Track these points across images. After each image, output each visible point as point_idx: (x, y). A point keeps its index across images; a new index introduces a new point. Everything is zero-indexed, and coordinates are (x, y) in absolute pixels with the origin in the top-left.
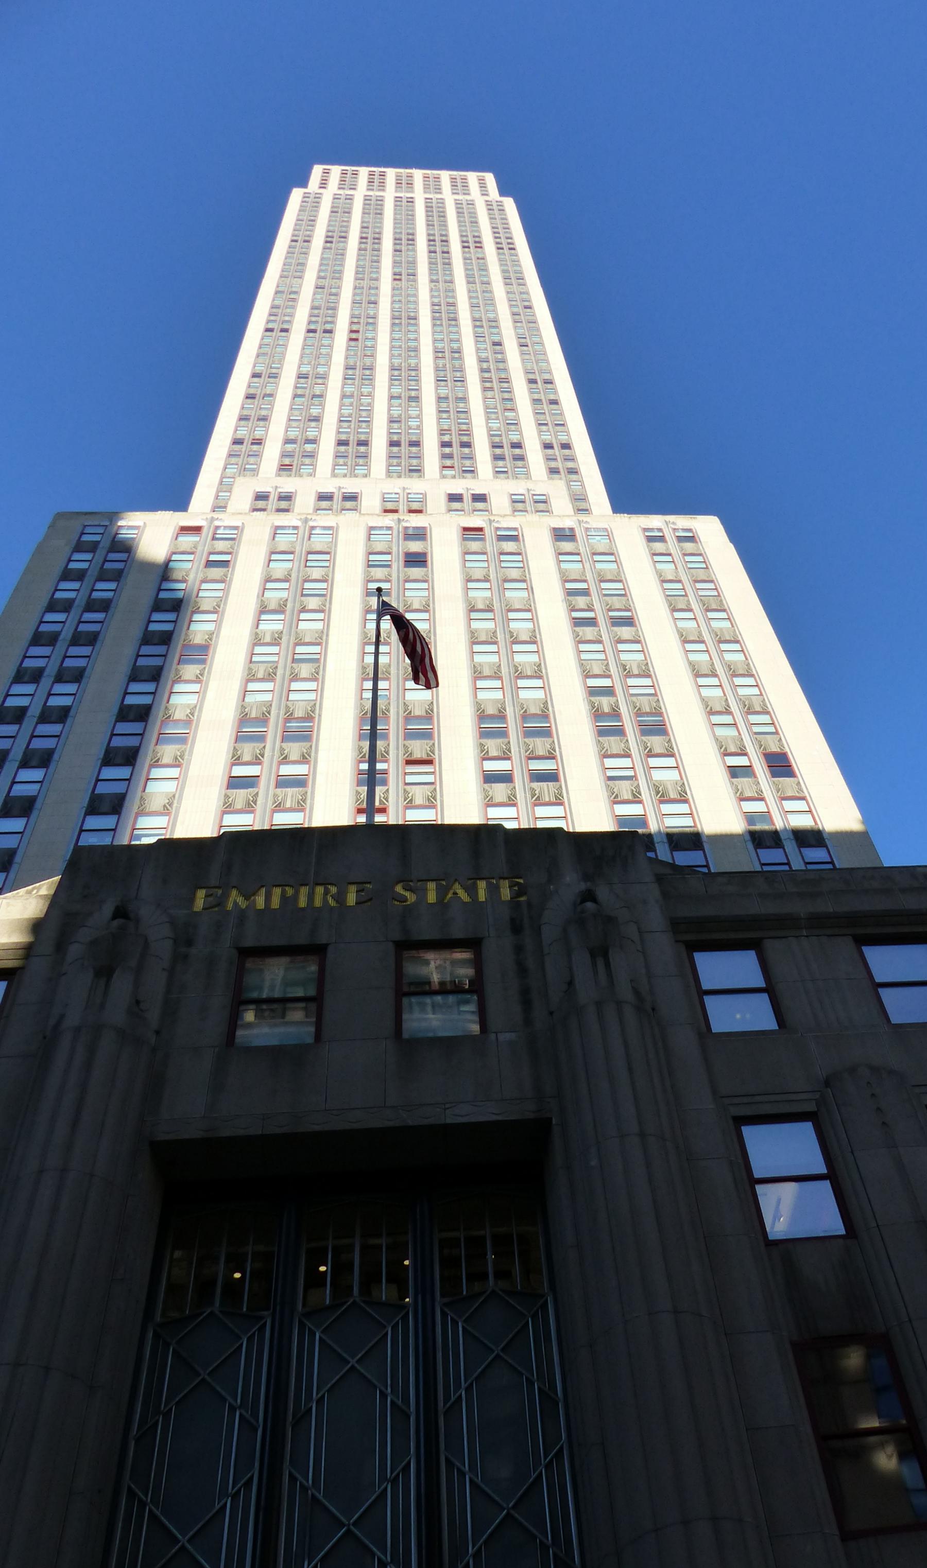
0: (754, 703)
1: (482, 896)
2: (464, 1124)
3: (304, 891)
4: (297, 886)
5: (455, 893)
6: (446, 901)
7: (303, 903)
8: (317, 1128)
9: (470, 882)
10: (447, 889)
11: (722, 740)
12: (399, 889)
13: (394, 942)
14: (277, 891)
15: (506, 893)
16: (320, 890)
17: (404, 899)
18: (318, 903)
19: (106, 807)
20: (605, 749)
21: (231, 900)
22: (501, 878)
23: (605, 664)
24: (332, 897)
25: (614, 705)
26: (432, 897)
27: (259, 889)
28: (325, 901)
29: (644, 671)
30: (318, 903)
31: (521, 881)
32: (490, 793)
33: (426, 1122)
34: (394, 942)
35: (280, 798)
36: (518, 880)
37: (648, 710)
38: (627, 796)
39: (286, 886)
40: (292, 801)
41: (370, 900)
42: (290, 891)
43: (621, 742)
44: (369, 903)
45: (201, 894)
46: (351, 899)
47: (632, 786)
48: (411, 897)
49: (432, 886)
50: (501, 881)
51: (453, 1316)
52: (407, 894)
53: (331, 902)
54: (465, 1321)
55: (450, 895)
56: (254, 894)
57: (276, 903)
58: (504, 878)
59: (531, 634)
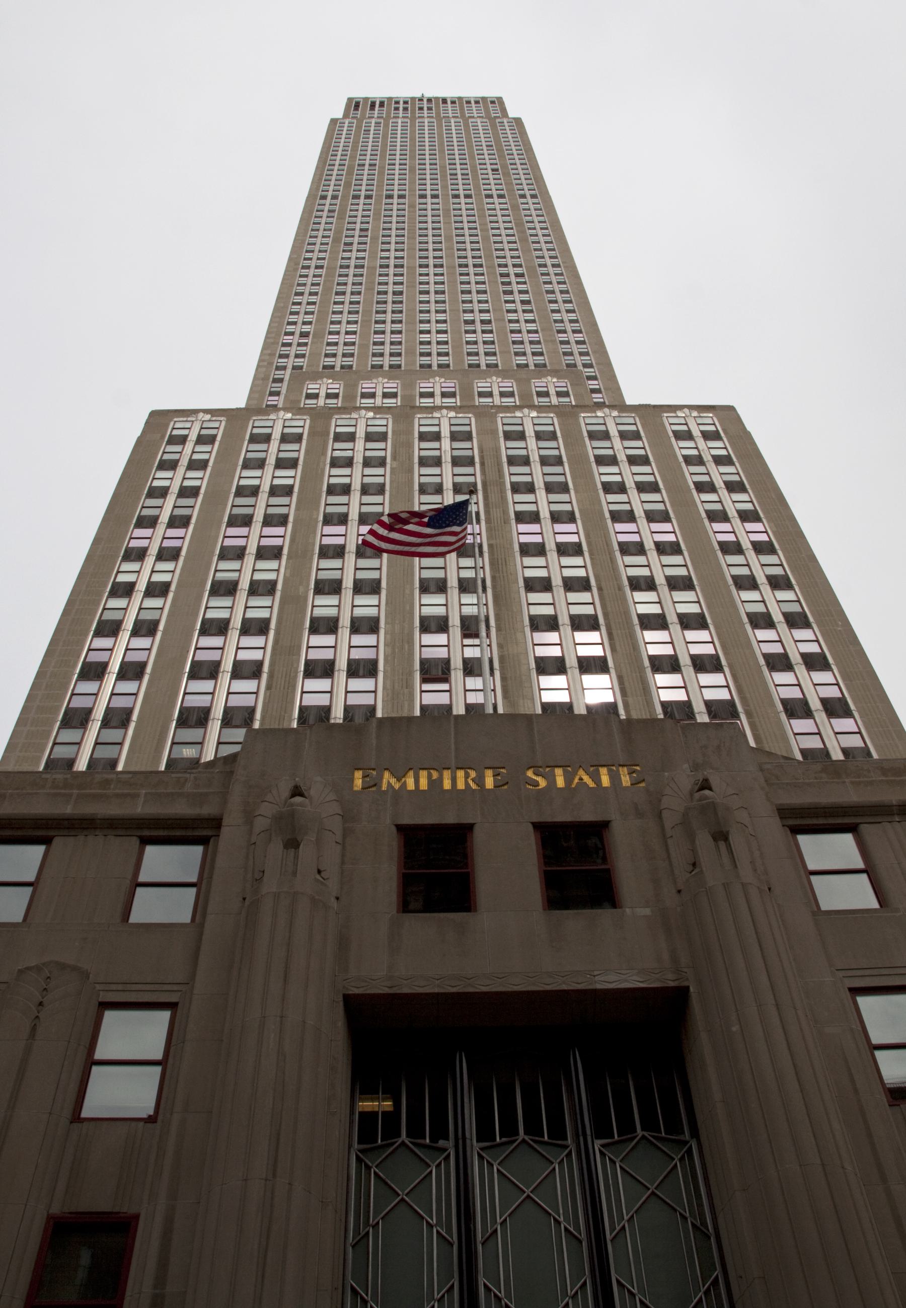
1: (605, 781)
2: (613, 989)
3: (447, 774)
4: (440, 771)
5: (581, 779)
6: (573, 786)
7: (447, 785)
8: (485, 989)
9: (592, 769)
10: (575, 773)
12: (530, 774)
13: (532, 823)
14: (423, 775)
15: (626, 780)
16: (460, 774)
17: (537, 784)
18: (461, 785)
19: (204, 673)
21: (385, 781)
22: (620, 765)
24: (473, 780)
26: (560, 782)
27: (408, 772)
28: (467, 784)
30: (461, 785)
31: (638, 768)
32: (542, 665)
33: (580, 987)
34: (532, 823)
35: (353, 667)
36: (635, 768)
39: (431, 769)
40: (364, 670)
41: (507, 783)
42: (435, 775)
44: (506, 787)
45: (358, 775)
46: (489, 783)
48: (543, 783)
49: (559, 772)
50: (620, 768)
51: (610, 1155)
52: (539, 779)
53: (473, 786)
54: (621, 1161)
55: (576, 780)
56: (404, 776)
57: (424, 784)
58: (623, 766)
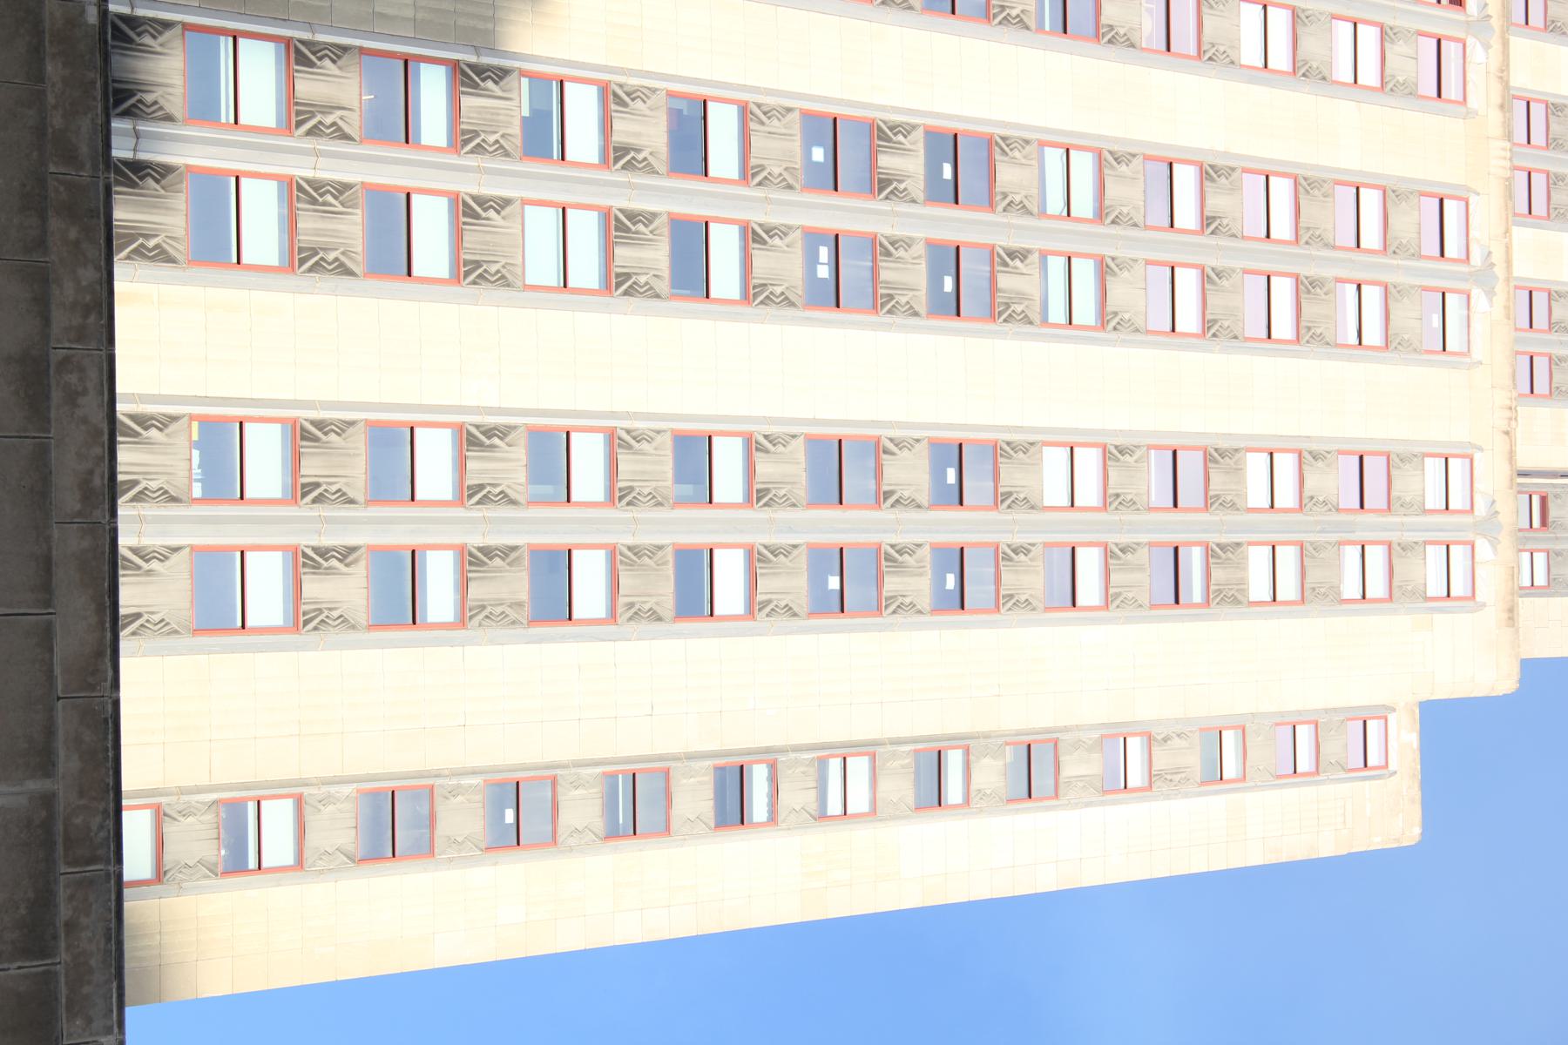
0: (907, 579)
11: (789, 448)
20: (763, 118)
23: (1026, 202)
25: (902, 186)
29: (1008, 306)
37: (884, 275)
38: (624, 130)
43: (786, 169)
47: (651, 154)
59: (1122, 32)
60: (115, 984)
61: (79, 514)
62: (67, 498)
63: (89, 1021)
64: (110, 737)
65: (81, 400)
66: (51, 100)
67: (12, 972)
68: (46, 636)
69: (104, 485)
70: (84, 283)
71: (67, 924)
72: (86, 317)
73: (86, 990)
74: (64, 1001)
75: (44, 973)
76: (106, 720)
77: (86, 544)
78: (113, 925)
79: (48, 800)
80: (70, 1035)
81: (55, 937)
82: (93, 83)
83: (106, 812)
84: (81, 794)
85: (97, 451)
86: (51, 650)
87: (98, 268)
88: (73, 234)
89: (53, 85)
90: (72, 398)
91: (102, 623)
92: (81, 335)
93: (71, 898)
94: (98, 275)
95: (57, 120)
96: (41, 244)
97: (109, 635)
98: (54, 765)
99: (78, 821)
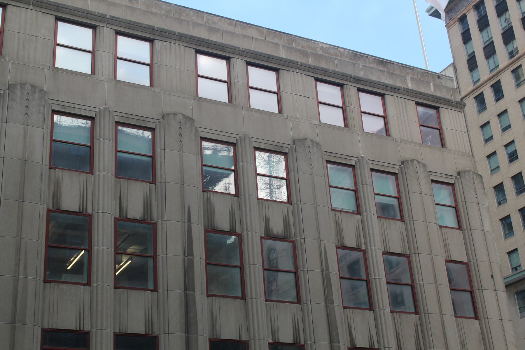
60: (311, 41)
61: (234, 27)
62: (231, 29)
63: (317, 47)
64: (272, 31)
65: (214, 21)
66: (160, 12)
67: (310, 60)
68: (256, 39)
69: (229, 21)
70: (193, 15)
71: (302, 48)
72: (199, 16)
73: (312, 47)
74: (314, 51)
75: (311, 54)
76: (269, 31)
77: (239, 27)
78: (302, 39)
79: (283, 46)
80: (319, 52)
81: (305, 51)
82: (155, 2)
83: (284, 35)
84: (281, 39)
85: (223, 20)
86: (259, 39)
87: (190, 11)
88: (184, 14)
89: (157, 11)
90: (214, 23)
91: (253, 28)
92: (202, 18)
93: (298, 46)
94: (191, 11)
95: (163, 12)
96: (188, 22)
97: (254, 27)
98: (277, 43)
99: (286, 41)
